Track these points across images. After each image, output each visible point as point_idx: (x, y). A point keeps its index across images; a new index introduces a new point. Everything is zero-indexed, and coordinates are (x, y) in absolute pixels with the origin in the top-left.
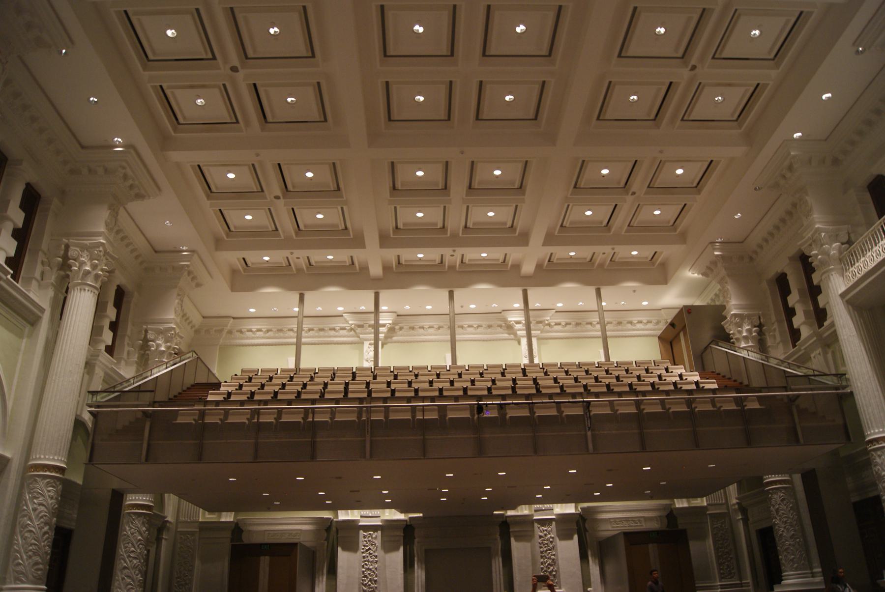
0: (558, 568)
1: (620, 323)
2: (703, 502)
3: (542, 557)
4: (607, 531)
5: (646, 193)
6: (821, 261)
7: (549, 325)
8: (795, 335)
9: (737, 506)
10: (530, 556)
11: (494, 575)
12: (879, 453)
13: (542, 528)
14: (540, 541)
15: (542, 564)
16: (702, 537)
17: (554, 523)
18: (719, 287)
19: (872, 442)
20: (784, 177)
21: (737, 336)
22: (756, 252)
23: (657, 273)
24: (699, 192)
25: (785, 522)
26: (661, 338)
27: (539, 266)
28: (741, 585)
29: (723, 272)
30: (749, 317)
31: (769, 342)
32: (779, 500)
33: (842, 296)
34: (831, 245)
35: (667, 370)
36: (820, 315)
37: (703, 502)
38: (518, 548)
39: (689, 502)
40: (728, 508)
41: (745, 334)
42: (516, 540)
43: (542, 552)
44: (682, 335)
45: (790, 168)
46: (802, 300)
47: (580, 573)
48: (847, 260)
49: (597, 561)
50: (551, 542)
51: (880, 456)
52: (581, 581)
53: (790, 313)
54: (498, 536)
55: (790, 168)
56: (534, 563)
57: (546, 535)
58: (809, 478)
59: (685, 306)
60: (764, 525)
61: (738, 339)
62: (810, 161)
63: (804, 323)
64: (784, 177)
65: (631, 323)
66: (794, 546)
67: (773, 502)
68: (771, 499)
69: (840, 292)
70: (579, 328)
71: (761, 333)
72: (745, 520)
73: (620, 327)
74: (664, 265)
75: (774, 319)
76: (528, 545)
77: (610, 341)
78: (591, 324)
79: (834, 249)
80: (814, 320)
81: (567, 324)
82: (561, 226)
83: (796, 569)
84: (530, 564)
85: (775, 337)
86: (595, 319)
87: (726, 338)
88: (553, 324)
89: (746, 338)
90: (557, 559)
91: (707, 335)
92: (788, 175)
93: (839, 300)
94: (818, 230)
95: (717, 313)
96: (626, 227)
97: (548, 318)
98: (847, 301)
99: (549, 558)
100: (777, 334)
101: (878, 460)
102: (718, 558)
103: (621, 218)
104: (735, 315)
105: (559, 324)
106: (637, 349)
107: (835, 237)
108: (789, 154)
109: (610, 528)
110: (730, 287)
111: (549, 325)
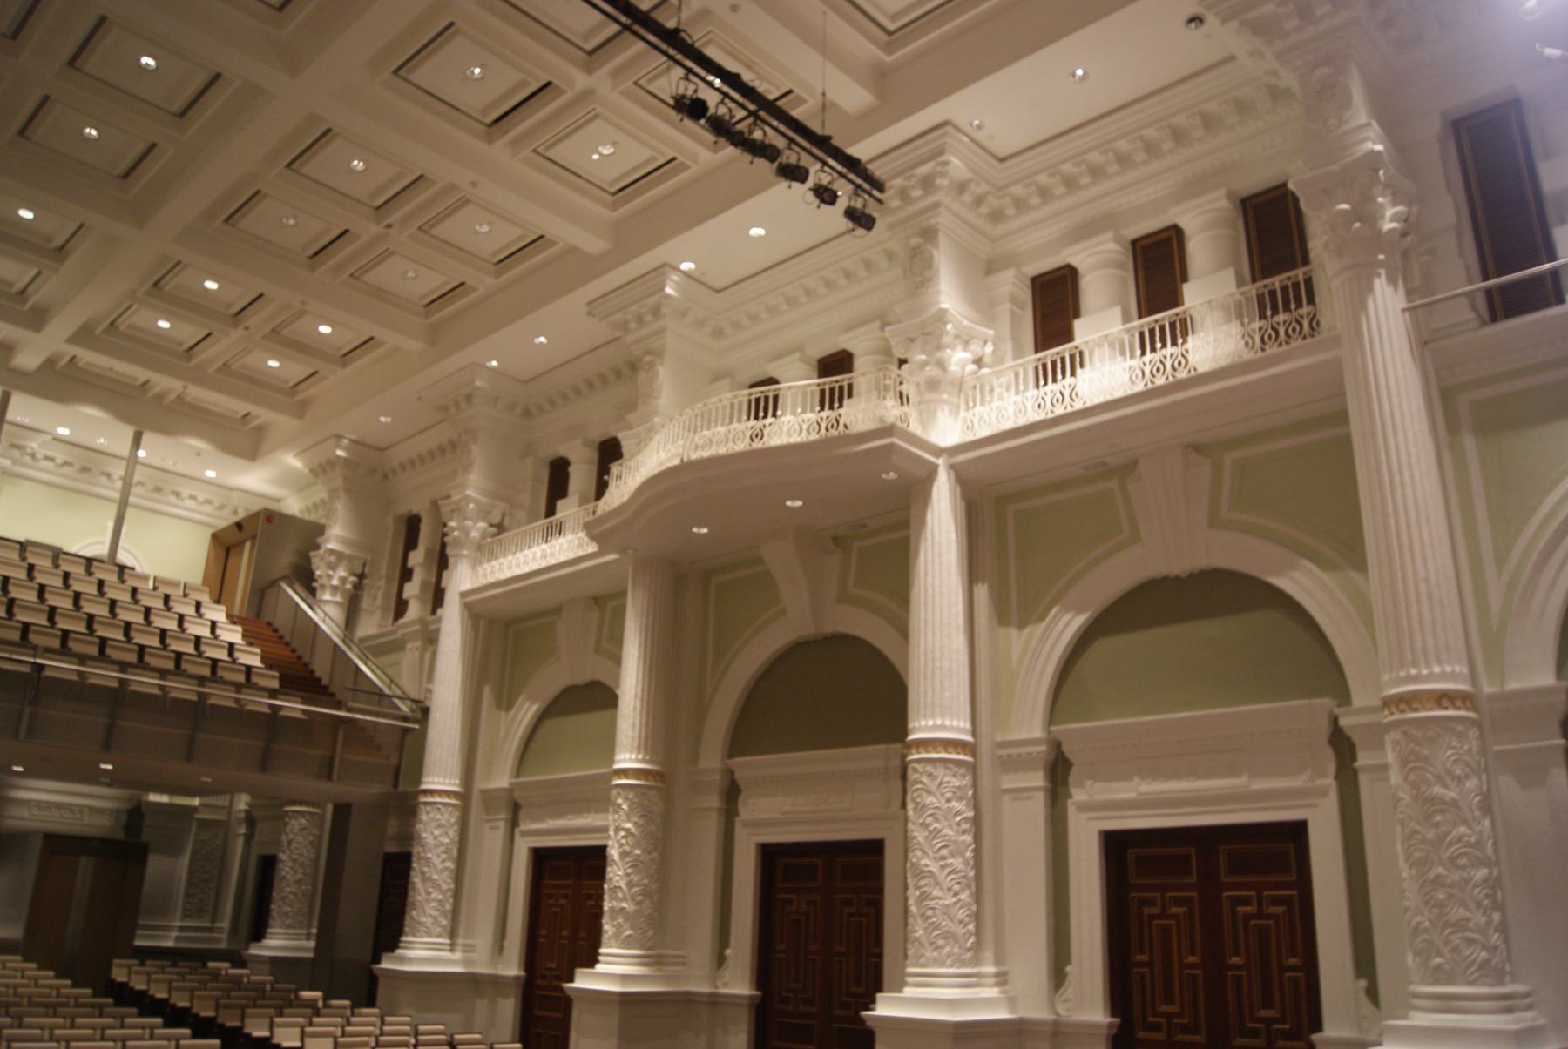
1: (158, 490)
2: (196, 802)
5: (265, 337)
6: (455, 539)
7: (33, 456)
8: (401, 607)
16: (176, 852)
18: (325, 495)
19: (426, 792)
20: (457, 404)
21: (324, 581)
22: (394, 471)
23: (247, 443)
24: (344, 365)
25: (295, 861)
26: (214, 536)
27: (50, 363)
28: (210, 930)
29: (339, 482)
30: (350, 559)
31: (365, 603)
32: (297, 828)
33: (463, 595)
34: (475, 522)
35: (198, 605)
36: (437, 597)
37: (196, 802)
40: (230, 813)
41: (335, 582)
44: (248, 545)
45: (469, 398)
46: (426, 564)
48: (486, 550)
53: (406, 574)
55: (469, 398)
58: (343, 812)
59: (266, 510)
60: (269, 851)
61: (323, 587)
62: (496, 400)
63: (416, 597)
64: (457, 404)
65: (177, 494)
68: (286, 824)
70: (85, 476)
71: (358, 587)
72: (249, 838)
73: (156, 496)
74: (260, 431)
75: (383, 572)
77: (130, 512)
78: (108, 475)
79: (477, 529)
80: (430, 597)
81: (66, 463)
82: (112, 323)
83: (288, 927)
85: (375, 597)
86: (119, 470)
87: (306, 579)
88: (39, 456)
89: (335, 588)
91: (285, 560)
92: (463, 405)
94: (467, 497)
95: (312, 534)
96: (219, 364)
97: (34, 445)
100: (380, 595)
101: (424, 817)
102: (190, 884)
103: (212, 353)
104: (332, 552)
105: (51, 459)
106: (166, 551)
107: (484, 513)
110: (340, 506)
111: (33, 456)
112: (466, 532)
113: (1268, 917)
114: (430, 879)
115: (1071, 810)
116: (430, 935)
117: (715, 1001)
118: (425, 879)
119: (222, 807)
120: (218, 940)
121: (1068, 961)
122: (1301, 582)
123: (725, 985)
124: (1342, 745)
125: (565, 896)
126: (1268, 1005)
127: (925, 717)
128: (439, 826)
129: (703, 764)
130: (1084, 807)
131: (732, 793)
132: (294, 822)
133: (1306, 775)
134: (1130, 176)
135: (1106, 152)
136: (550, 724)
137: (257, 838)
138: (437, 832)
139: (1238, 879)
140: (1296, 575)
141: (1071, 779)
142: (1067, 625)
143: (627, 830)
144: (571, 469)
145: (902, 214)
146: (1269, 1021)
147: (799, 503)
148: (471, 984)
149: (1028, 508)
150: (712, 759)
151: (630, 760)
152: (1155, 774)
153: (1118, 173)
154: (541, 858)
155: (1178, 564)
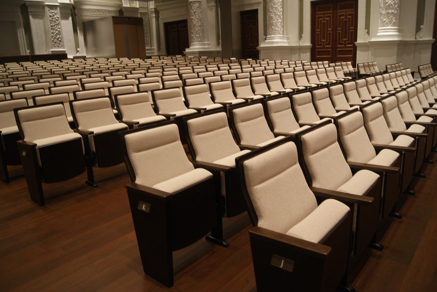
0: (62, 36)
3: (52, 29)
4: (88, 16)
9: (153, 10)
10: (43, 28)
11: (19, 39)
13: (51, 11)
14: (50, 19)
15: (52, 33)
17: (58, 8)
25: (198, 19)
38: (35, 23)
39: (130, 4)
40: (148, 11)
42: (33, 17)
43: (52, 26)
47: (73, 39)
49: (82, 34)
50: (57, 20)
52: (74, 44)
54: (21, 15)
56: (46, 32)
57: (54, 15)
66: (200, 30)
67: (193, 8)
68: (192, 6)
72: (157, 18)
76: (41, 21)
83: (200, 41)
84: (43, 33)
90: (62, 31)
99: (57, 30)
109: (89, 15)
114: (277, 14)
116: (280, 34)
117: (417, 43)
118: (275, 15)
119: (145, 8)
120: (154, 53)
123: (421, 38)
125: (329, 17)
132: (195, 5)
137: (161, 17)
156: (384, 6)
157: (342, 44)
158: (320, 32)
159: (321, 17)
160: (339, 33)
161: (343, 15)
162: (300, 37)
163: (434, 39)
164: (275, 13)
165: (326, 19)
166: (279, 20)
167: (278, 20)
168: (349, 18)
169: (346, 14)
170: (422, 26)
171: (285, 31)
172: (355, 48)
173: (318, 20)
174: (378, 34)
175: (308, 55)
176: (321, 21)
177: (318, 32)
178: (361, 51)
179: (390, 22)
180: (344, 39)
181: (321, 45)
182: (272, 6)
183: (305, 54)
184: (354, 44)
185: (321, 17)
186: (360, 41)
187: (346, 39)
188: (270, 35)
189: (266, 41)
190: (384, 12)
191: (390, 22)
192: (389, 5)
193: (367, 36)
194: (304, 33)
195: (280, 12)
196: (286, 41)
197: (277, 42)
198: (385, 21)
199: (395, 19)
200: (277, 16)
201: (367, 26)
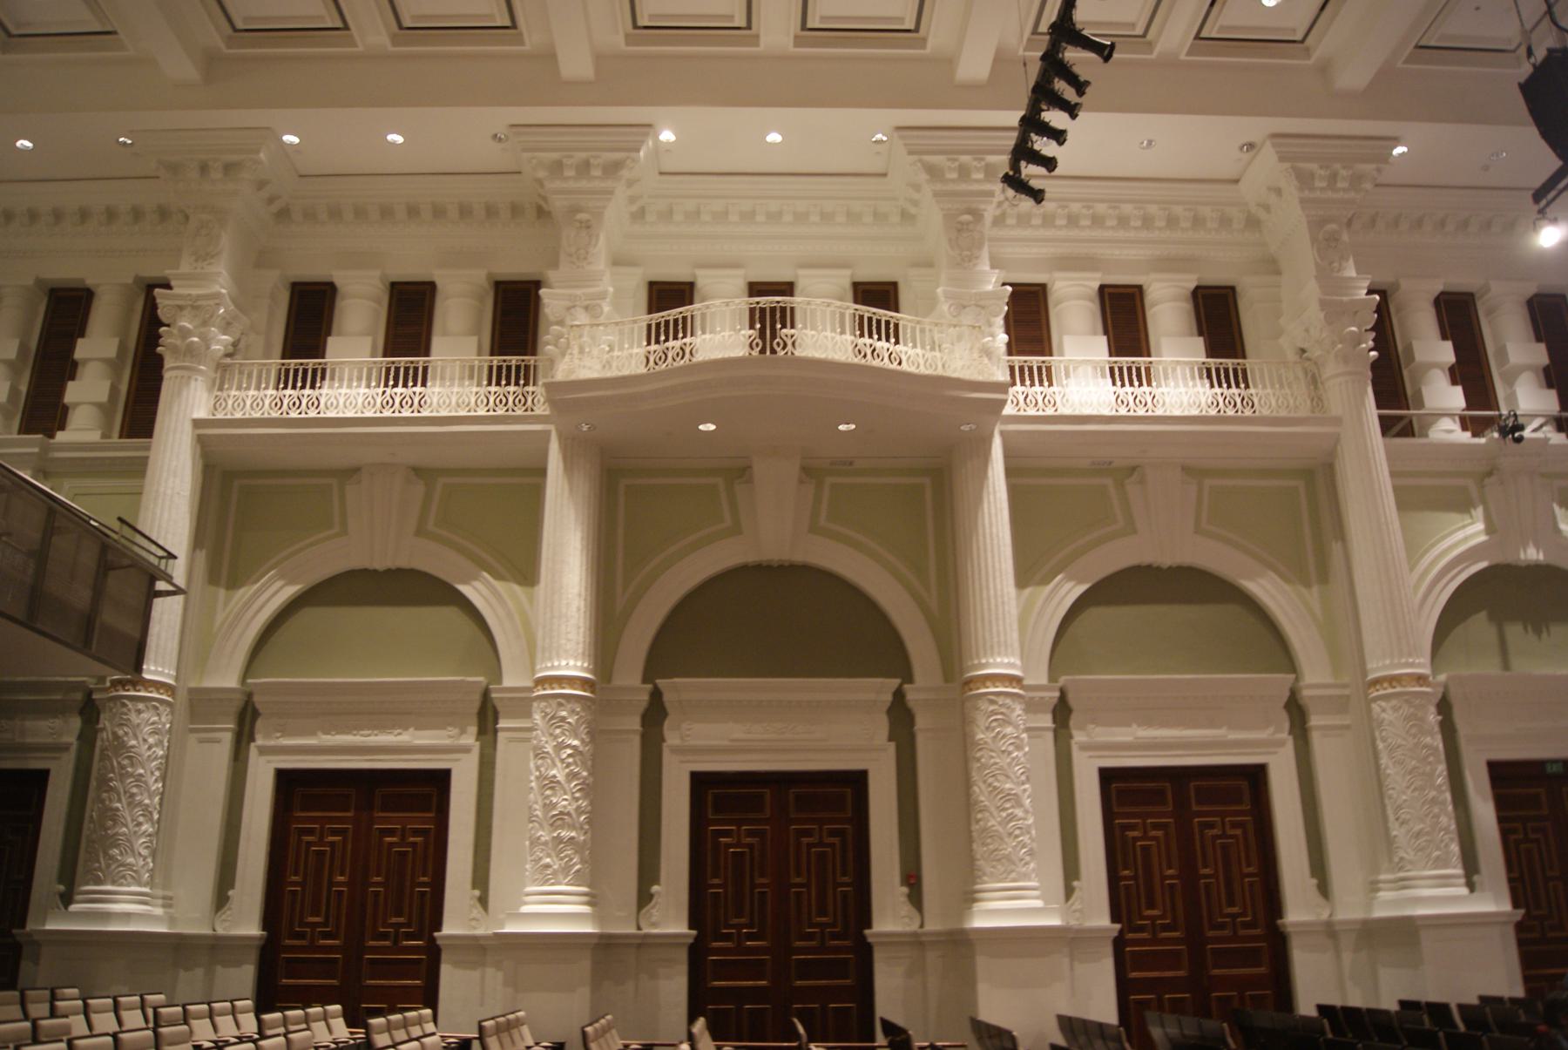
12: (141, 706)
33: (197, 423)
51: (139, 712)
55: (229, 168)
64: (204, 169)
69: (196, 416)
79: (220, 341)
92: (217, 175)
93: (188, 427)
98: (199, 436)
108: (258, 152)
112: (206, 341)
113: (1231, 837)
114: (140, 803)
115: (1075, 748)
116: (140, 885)
117: (643, 944)
118: (132, 804)
121: (1077, 877)
122: (1266, 589)
123: (654, 925)
124: (1296, 711)
126: (1231, 903)
127: (999, 654)
128: (154, 733)
129: (618, 681)
130: (1084, 747)
131: (655, 714)
133: (1271, 730)
134: (1121, 234)
135: (1089, 208)
136: (309, 615)
138: (151, 740)
139: (1205, 808)
140: (1262, 581)
141: (1072, 723)
142: (1069, 591)
143: (574, 747)
144: (341, 304)
145: (951, 187)
146: (1234, 916)
147: (712, 427)
148: (175, 950)
149: (1071, 484)
150: (629, 675)
151: (575, 667)
152: (1148, 723)
153: (1112, 228)
154: (294, 788)
155: (1166, 558)
156: (546, 813)
157: (384, 936)
158: (303, 884)
159: (311, 832)
160: (376, 894)
161: (391, 832)
162: (221, 899)
163: (694, 932)
164: (132, 796)
165: (331, 839)
166: (144, 828)
167: (139, 824)
168: (414, 844)
169: (403, 830)
170: (655, 888)
171: (162, 875)
172: (434, 954)
173: (300, 841)
174: (525, 909)
175: (244, 976)
176: (309, 844)
177: (295, 884)
178: (457, 964)
179: (566, 869)
180: (394, 920)
181: (301, 936)
182: (123, 767)
183: (233, 972)
184: (434, 939)
185: (311, 832)
186: (451, 927)
187: (401, 920)
188: (99, 882)
189: (74, 907)
190: (544, 835)
191: (566, 869)
192: (561, 813)
193: (477, 911)
194: (238, 884)
195: (151, 797)
196: (159, 911)
197: (127, 916)
198: (548, 866)
199: (582, 861)
200: (138, 811)
201: (481, 878)
